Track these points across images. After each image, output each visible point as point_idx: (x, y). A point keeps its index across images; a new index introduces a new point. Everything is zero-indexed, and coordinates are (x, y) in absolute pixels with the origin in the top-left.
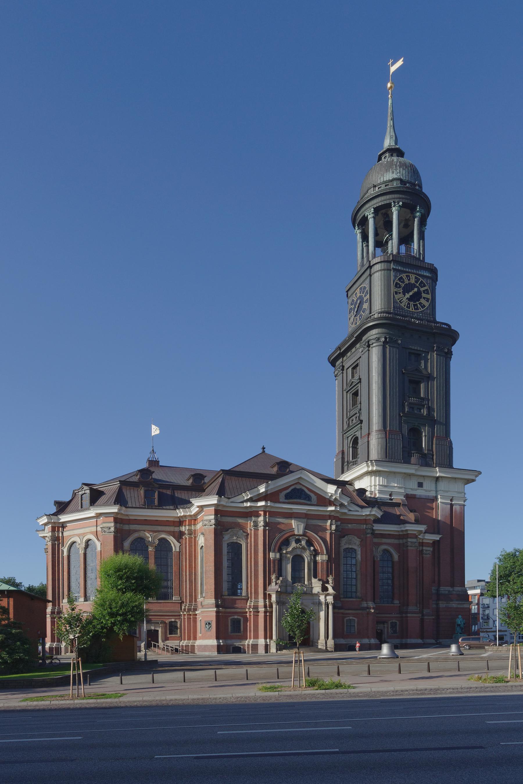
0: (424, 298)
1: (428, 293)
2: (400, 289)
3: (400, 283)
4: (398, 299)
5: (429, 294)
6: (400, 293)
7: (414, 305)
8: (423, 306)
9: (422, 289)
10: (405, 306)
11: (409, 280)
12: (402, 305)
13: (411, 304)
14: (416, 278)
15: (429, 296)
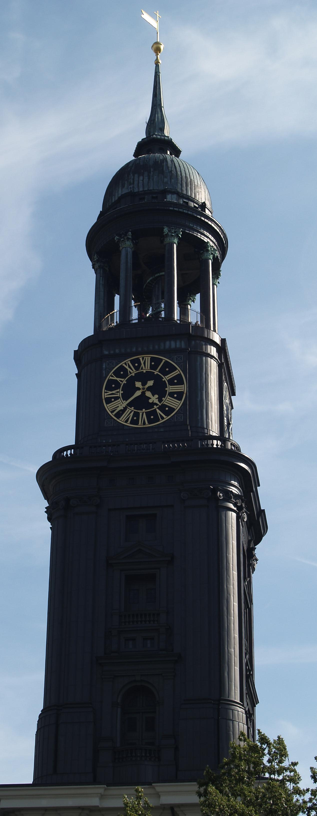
0: (171, 395)
1: (181, 382)
2: (118, 390)
3: (118, 379)
4: (112, 412)
5: (183, 383)
6: (116, 398)
7: (148, 415)
8: (172, 410)
9: (166, 379)
10: (126, 421)
11: (137, 368)
12: (121, 420)
13: (141, 414)
14: (152, 359)
15: (183, 388)
